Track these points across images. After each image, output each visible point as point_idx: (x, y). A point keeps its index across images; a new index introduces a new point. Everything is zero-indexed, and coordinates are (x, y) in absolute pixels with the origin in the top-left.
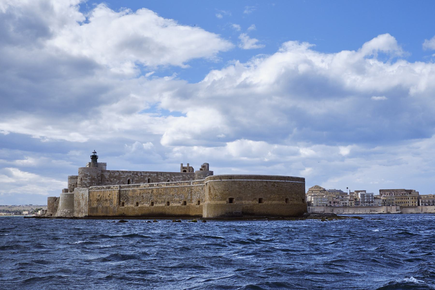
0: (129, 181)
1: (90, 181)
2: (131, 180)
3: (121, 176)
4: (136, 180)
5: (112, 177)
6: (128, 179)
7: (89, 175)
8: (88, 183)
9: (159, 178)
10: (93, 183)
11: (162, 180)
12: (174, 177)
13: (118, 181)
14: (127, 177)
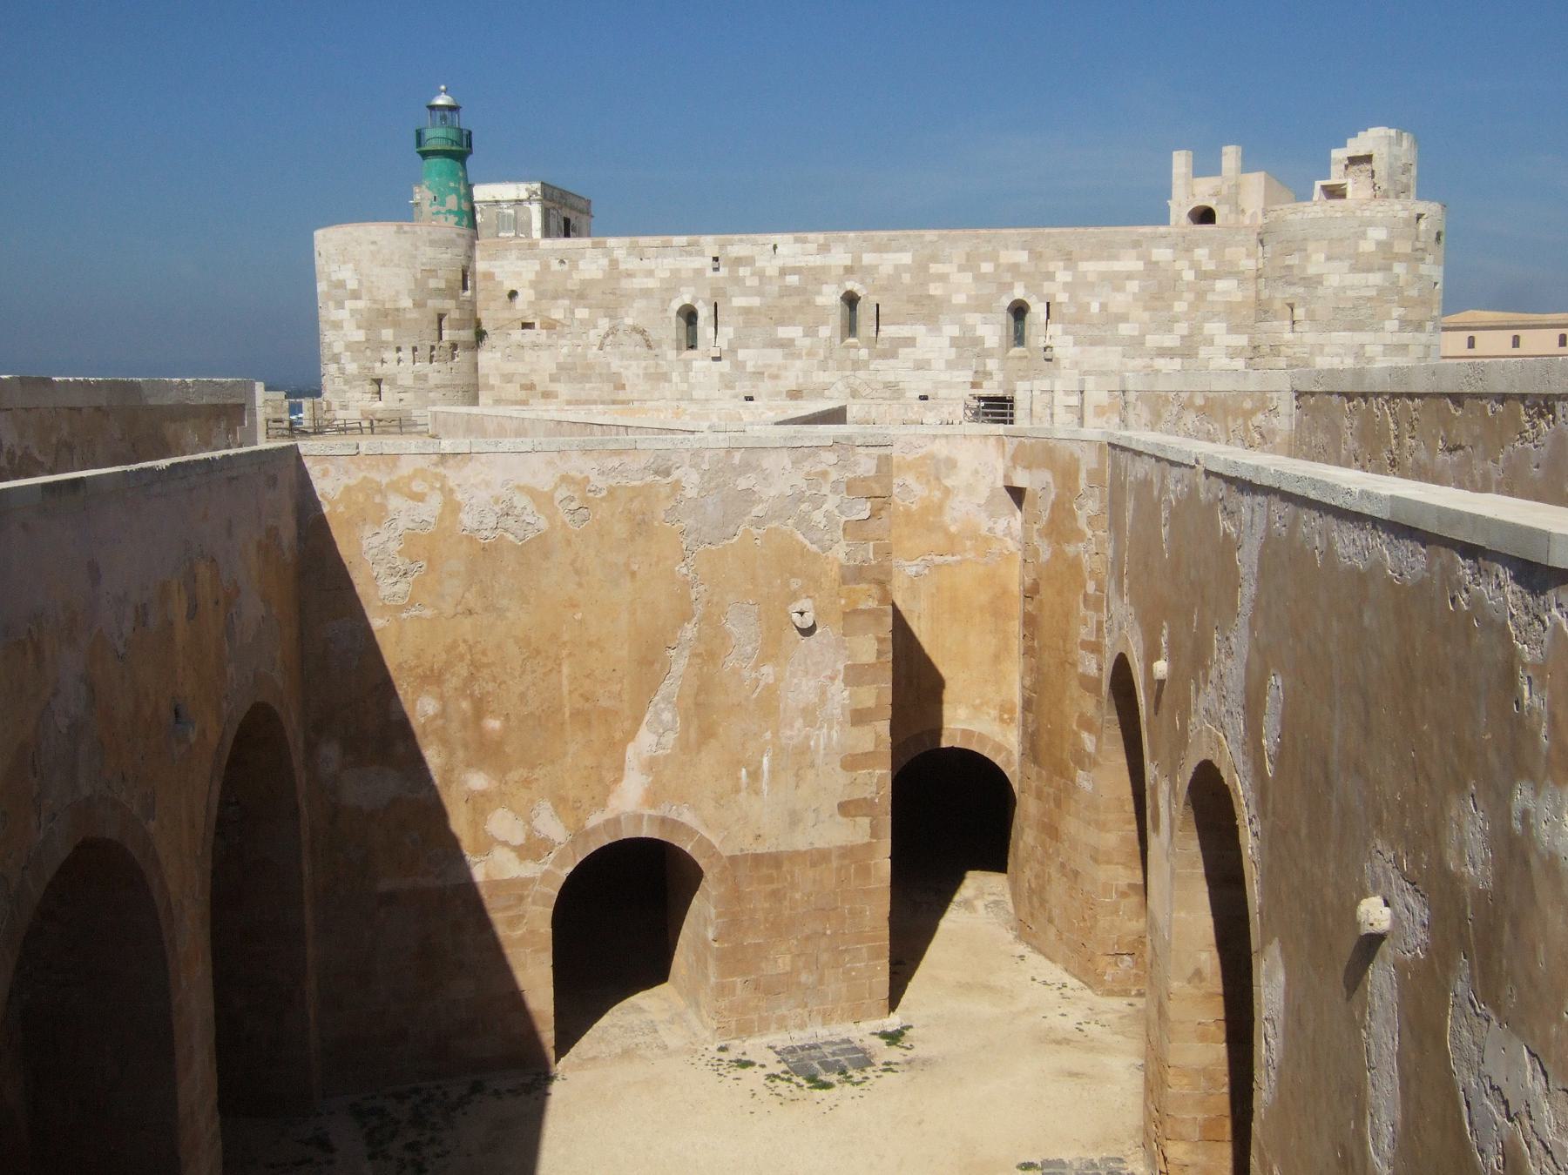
0: (689, 316)
1: (360, 336)
2: (704, 313)
3: (625, 284)
4: (747, 311)
5: (556, 297)
6: (676, 305)
7: (352, 285)
8: (348, 346)
9: (935, 289)
10: (383, 345)
11: (960, 299)
12: (1063, 276)
13: (604, 324)
14: (673, 284)
